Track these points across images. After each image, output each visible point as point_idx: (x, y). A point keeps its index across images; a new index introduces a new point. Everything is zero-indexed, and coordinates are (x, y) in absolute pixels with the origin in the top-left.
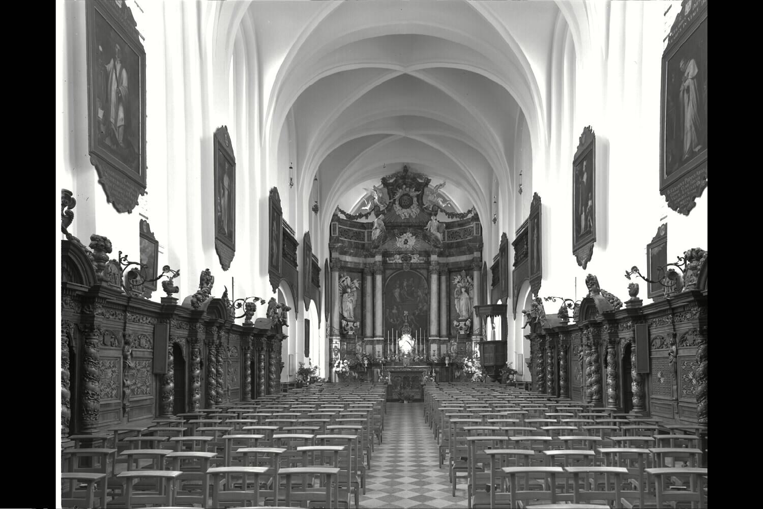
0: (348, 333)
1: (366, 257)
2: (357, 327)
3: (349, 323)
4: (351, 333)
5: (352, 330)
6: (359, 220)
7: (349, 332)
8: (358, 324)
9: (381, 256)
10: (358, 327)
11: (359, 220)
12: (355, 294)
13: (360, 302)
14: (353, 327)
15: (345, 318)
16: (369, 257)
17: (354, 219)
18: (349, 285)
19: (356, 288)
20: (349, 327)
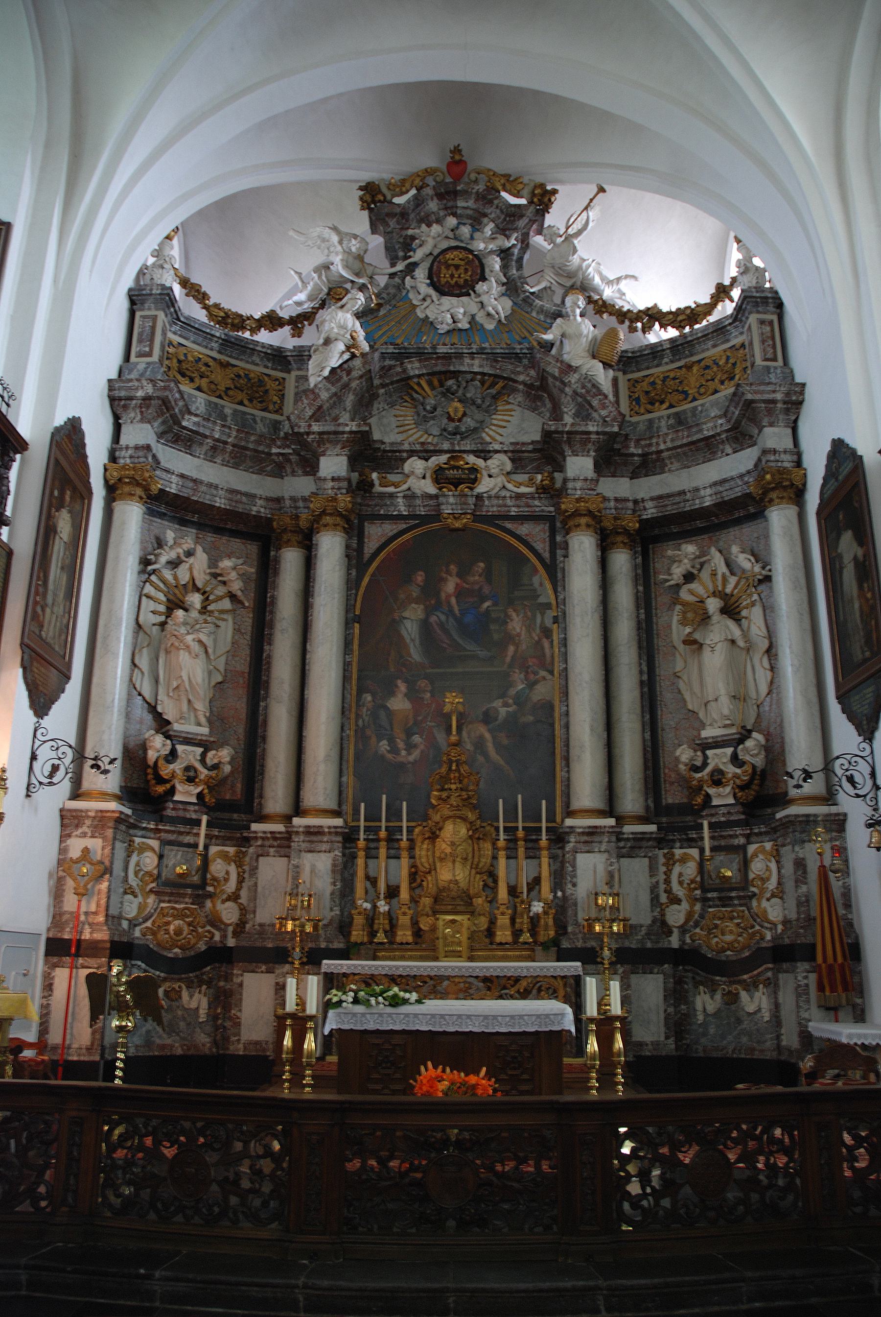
0: (172, 791)
1: (279, 471)
2: (216, 767)
3: (180, 748)
4: (185, 793)
5: (191, 780)
6: (264, 337)
7: (179, 787)
8: (225, 754)
9: (344, 460)
10: (227, 769)
11: (264, 337)
12: (227, 628)
13: (243, 664)
14: (198, 766)
15: (168, 723)
16: (293, 473)
17: (243, 328)
18: (199, 584)
19: (232, 597)
20: (177, 767)
